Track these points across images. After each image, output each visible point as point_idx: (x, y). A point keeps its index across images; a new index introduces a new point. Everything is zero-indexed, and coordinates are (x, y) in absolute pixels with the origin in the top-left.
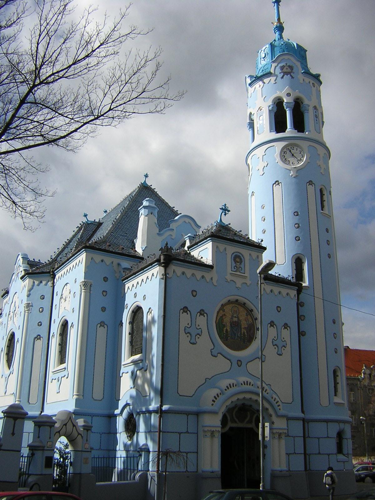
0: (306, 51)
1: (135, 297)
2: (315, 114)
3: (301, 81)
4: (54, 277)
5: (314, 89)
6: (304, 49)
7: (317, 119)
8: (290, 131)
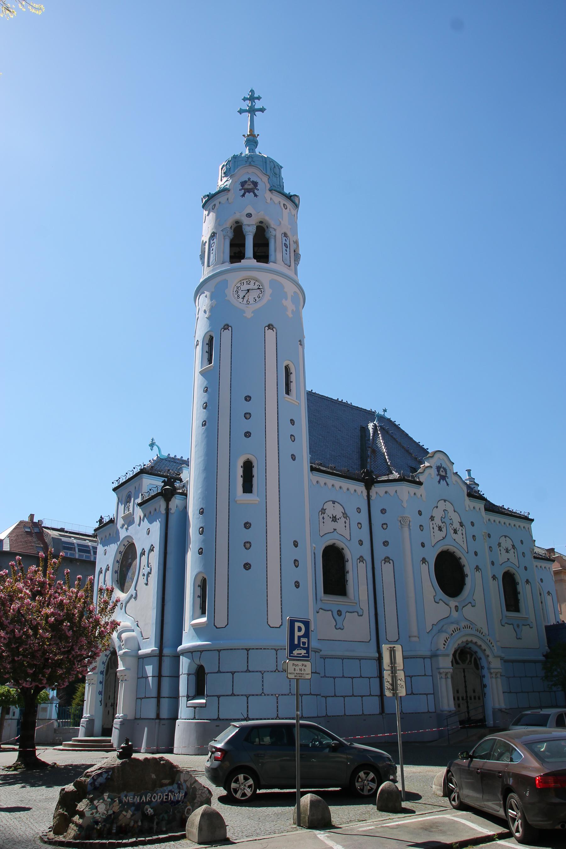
0: (281, 167)
3: (269, 201)
5: (286, 212)
6: (278, 165)
7: (288, 249)
8: (249, 262)
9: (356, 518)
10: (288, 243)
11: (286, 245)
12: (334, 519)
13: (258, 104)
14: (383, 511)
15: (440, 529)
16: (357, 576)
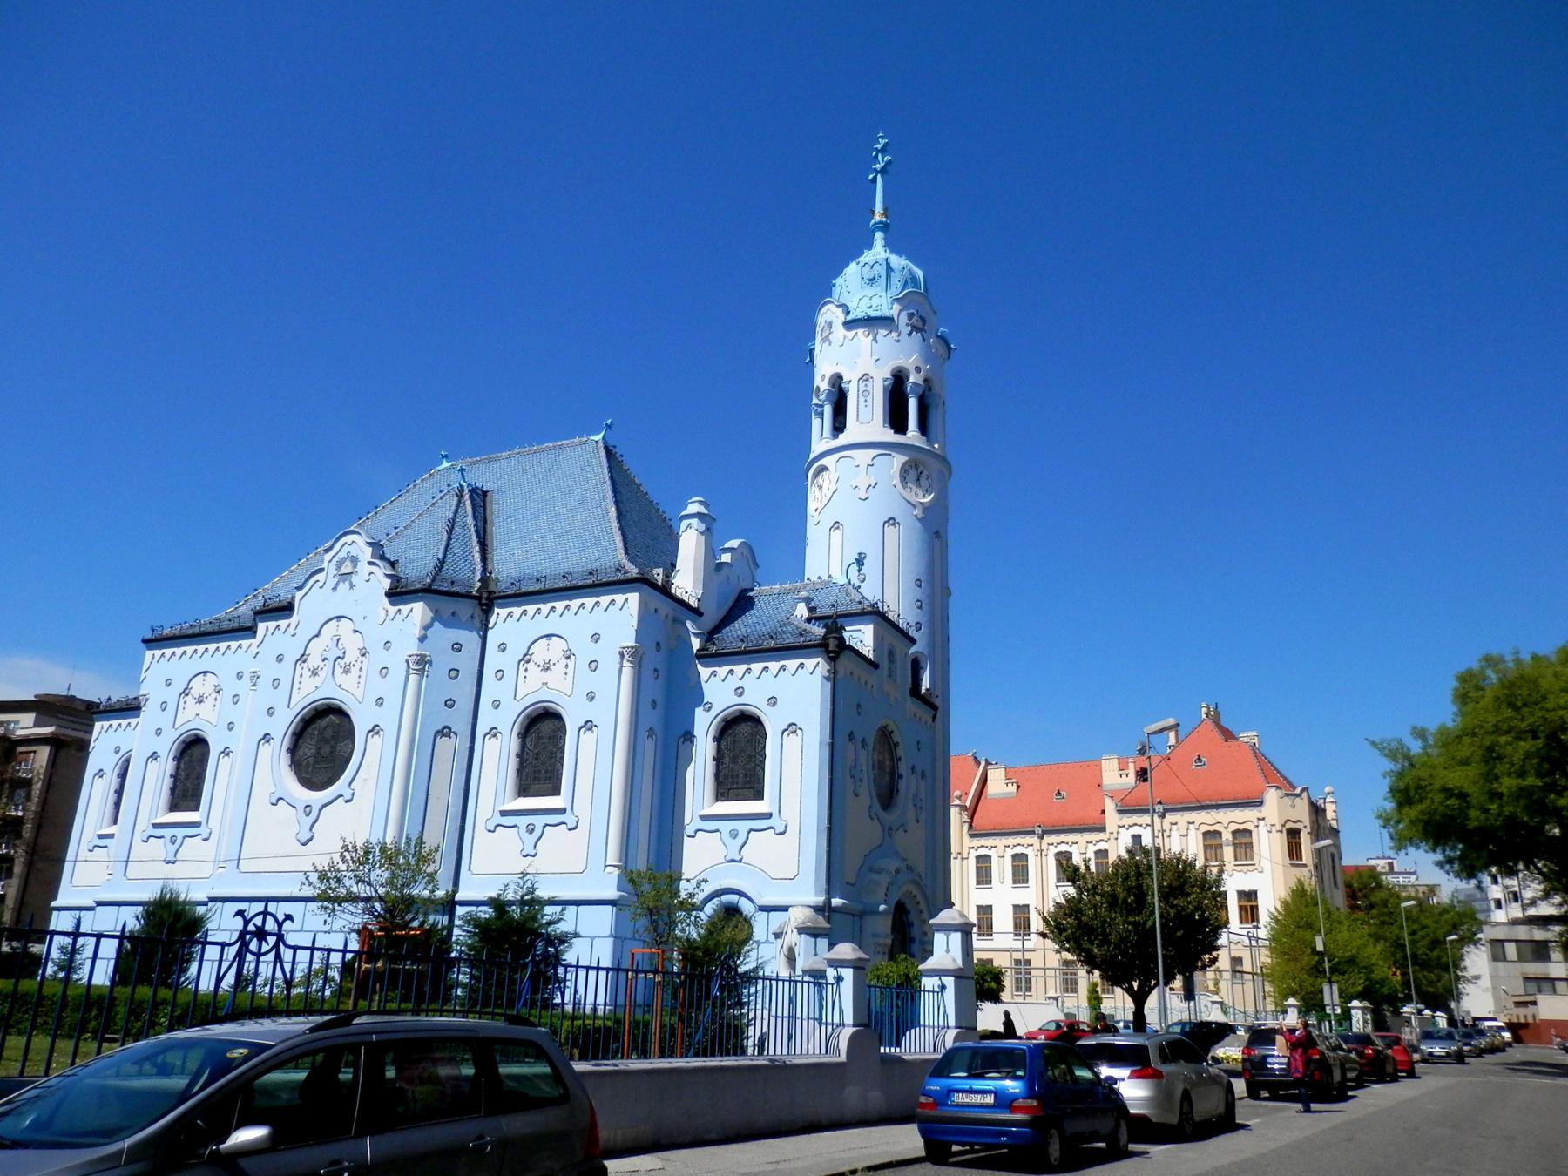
1: (741, 695)
4: (487, 611)
8: (913, 435)
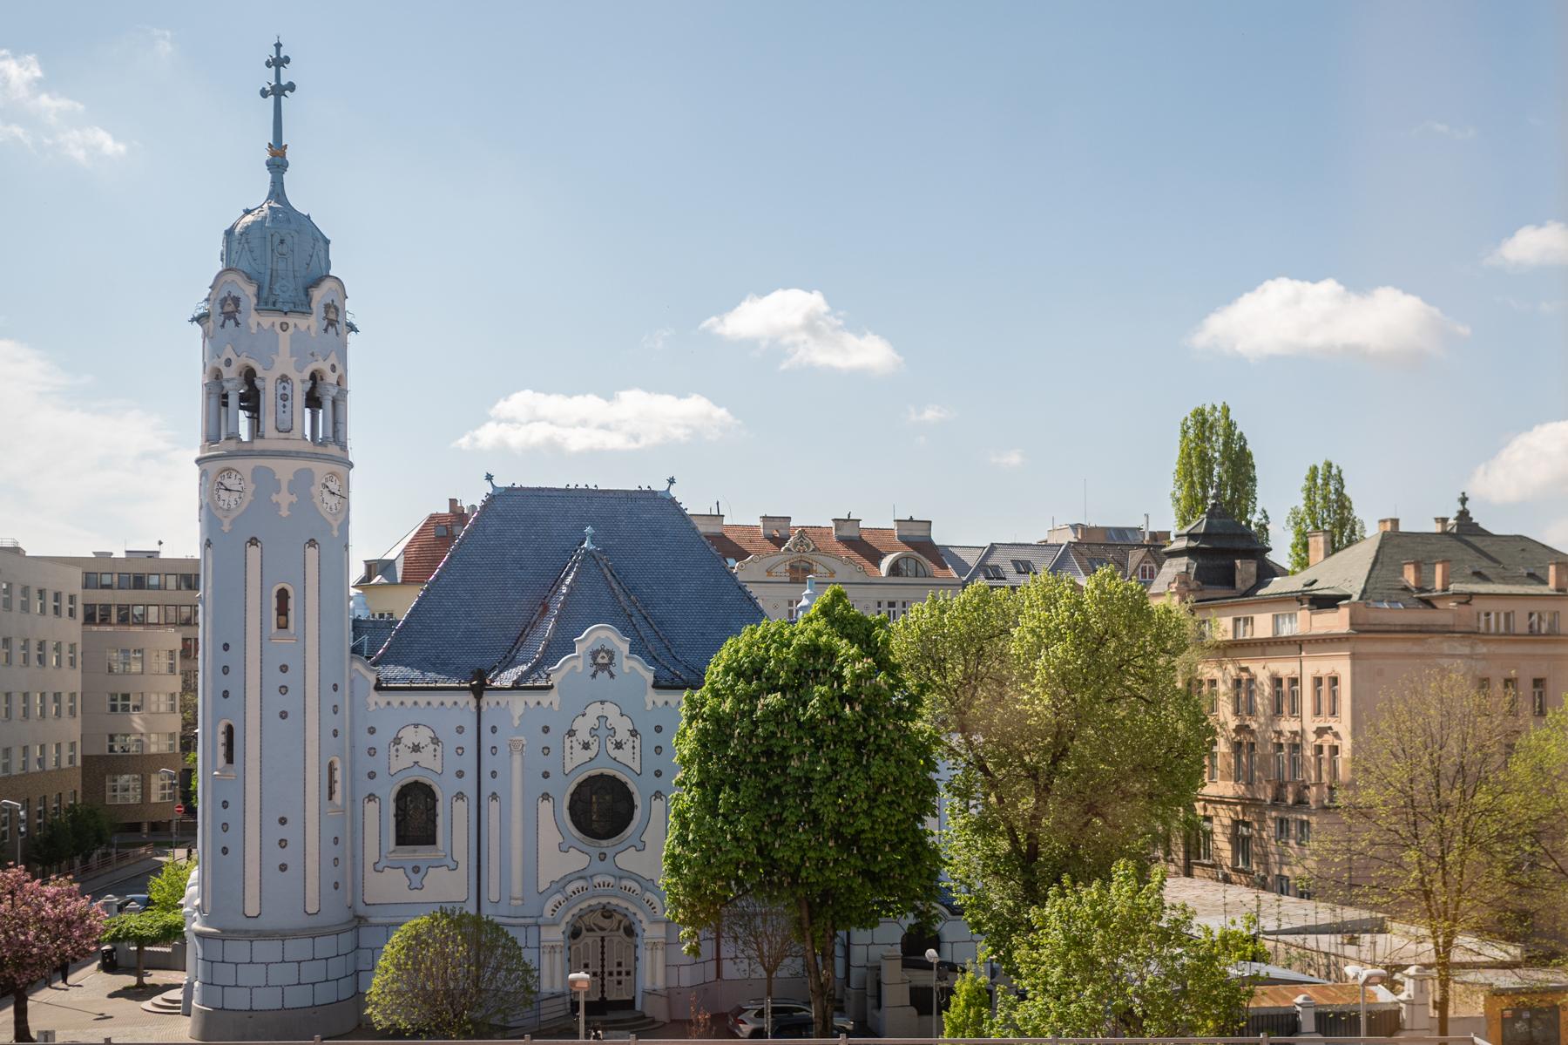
2: (281, 391)
9: (451, 740)
10: (288, 392)
11: (284, 398)
12: (416, 748)
13: (286, 76)
14: (494, 730)
15: (586, 746)
16: (453, 820)
